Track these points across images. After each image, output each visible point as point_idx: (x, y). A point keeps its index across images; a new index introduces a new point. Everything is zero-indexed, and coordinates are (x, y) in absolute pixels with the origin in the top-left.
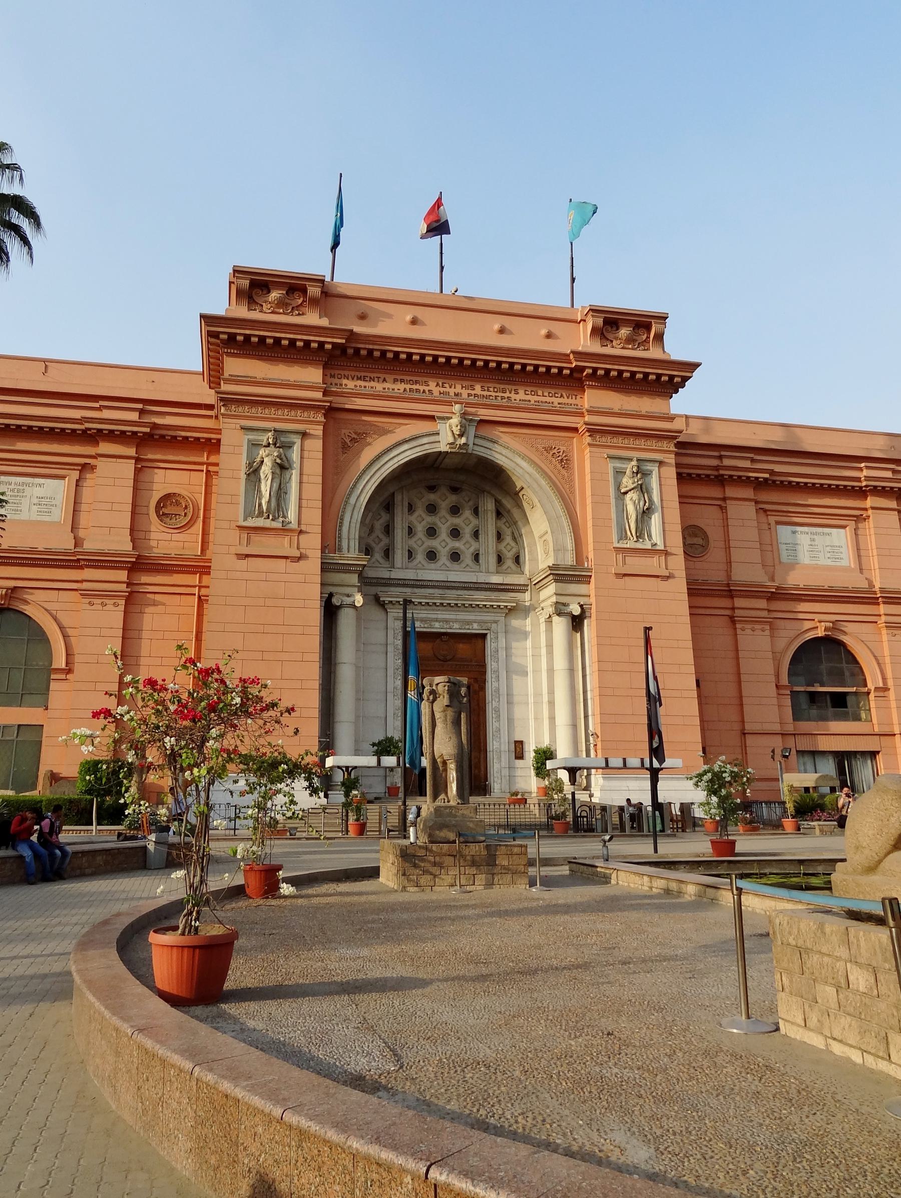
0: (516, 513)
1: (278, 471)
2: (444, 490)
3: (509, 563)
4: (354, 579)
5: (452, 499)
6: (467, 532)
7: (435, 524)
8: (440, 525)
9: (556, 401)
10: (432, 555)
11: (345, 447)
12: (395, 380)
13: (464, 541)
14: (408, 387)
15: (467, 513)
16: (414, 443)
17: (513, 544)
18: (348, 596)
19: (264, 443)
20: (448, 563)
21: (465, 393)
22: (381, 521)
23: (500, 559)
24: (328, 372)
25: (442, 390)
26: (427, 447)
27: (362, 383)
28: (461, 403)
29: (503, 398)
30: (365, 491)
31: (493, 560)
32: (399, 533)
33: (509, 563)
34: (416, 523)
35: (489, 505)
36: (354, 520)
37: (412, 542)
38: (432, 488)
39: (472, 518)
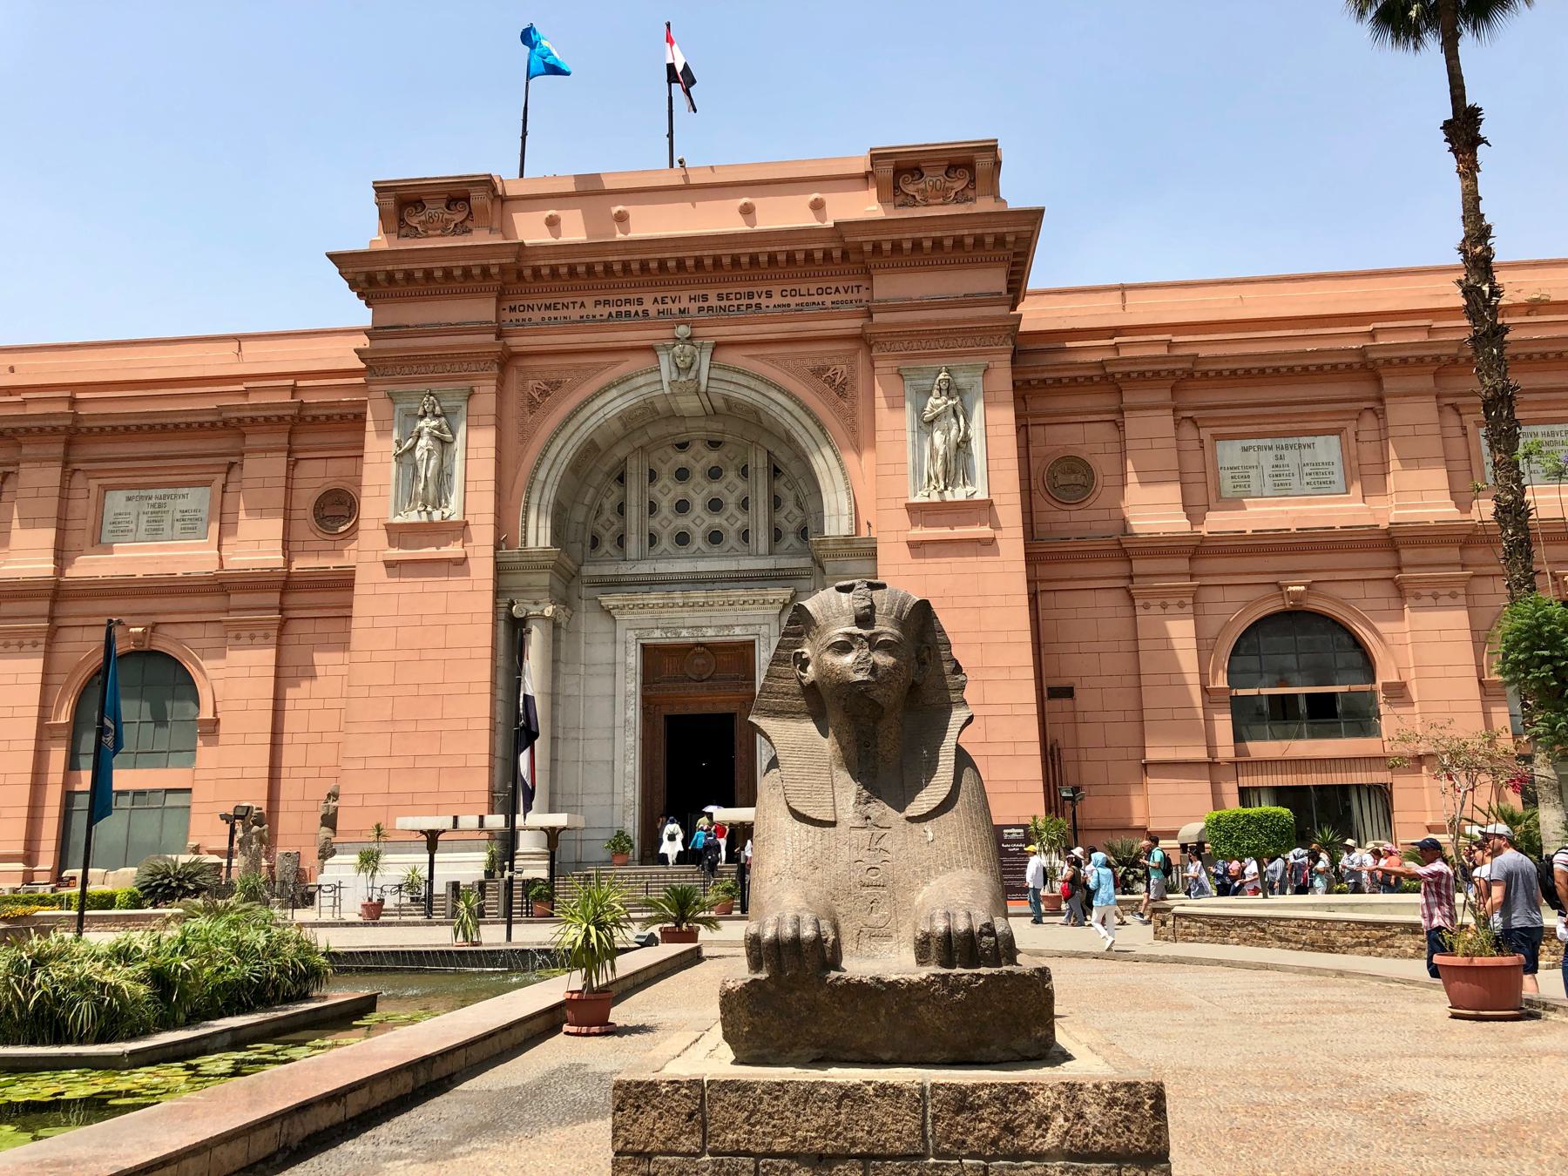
0: (794, 468)
1: (438, 443)
2: (698, 447)
3: (790, 540)
4: (544, 579)
5: (713, 457)
6: (731, 501)
7: (686, 494)
8: (692, 493)
9: (828, 299)
10: (683, 539)
11: (533, 405)
12: (597, 303)
13: (728, 513)
14: (614, 310)
15: (731, 476)
16: (624, 387)
17: (796, 511)
18: (536, 603)
19: (420, 412)
20: (703, 547)
21: (694, 306)
22: (613, 498)
23: (776, 535)
24: (506, 305)
25: (661, 307)
26: (644, 390)
27: (552, 314)
28: (686, 324)
29: (749, 306)
30: (559, 461)
31: (762, 539)
32: (633, 513)
33: (790, 540)
34: (659, 495)
35: (759, 461)
36: (544, 502)
37: (655, 523)
38: (683, 446)
39: (738, 482)
